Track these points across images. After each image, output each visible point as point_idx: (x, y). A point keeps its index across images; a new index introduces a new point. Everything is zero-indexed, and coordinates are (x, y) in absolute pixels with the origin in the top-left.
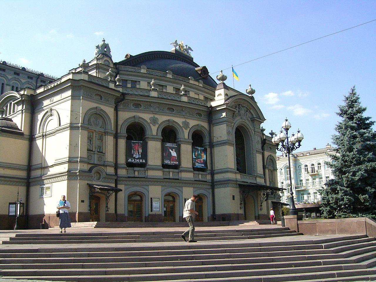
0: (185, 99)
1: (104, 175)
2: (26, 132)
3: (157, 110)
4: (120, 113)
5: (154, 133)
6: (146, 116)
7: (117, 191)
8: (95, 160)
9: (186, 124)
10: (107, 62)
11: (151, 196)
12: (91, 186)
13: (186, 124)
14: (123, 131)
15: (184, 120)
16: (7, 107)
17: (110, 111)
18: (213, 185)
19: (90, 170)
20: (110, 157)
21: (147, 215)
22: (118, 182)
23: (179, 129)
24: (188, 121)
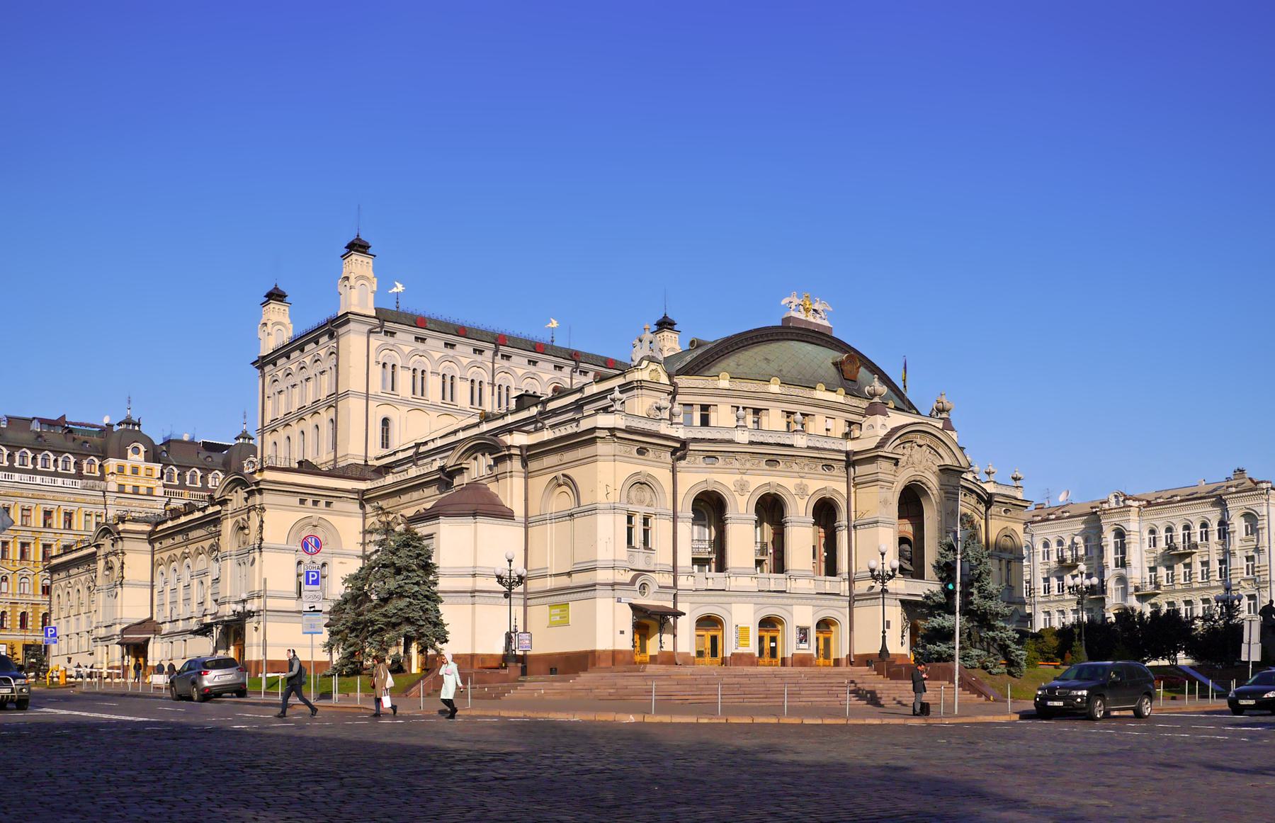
0: (800, 441)
1: (653, 588)
2: (519, 512)
3: (748, 465)
4: (679, 475)
5: (742, 509)
6: (723, 479)
7: (677, 614)
8: (640, 562)
9: (802, 490)
10: (654, 374)
11: (735, 622)
12: (633, 606)
13: (801, 490)
14: (686, 510)
15: (798, 481)
16: (475, 459)
17: (663, 476)
18: (853, 599)
19: (633, 582)
20: (662, 556)
21: (729, 655)
22: (679, 598)
23: (788, 500)
24: (805, 481)
